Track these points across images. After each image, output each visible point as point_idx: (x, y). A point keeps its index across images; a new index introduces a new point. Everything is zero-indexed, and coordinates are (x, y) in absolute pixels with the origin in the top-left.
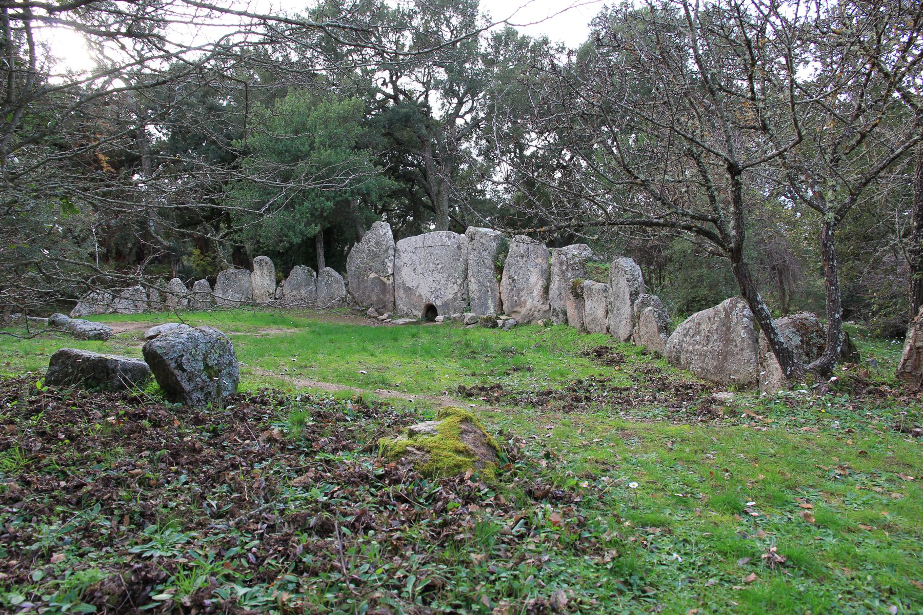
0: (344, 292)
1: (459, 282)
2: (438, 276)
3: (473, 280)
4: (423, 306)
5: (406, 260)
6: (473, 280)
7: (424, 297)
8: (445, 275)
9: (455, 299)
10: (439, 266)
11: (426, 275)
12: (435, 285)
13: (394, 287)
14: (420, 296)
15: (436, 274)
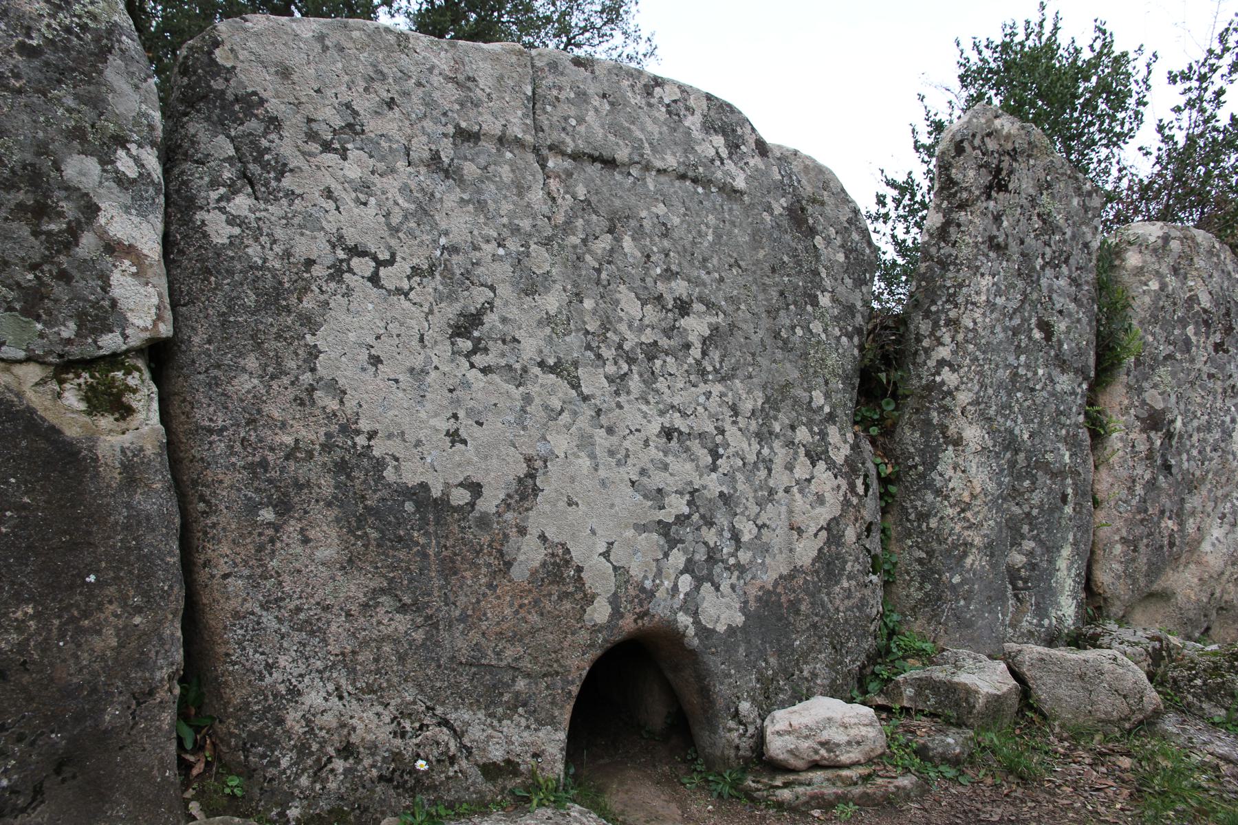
3: (973, 434)
4: (578, 664)
7: (599, 576)
10: (696, 326)
11: (594, 382)
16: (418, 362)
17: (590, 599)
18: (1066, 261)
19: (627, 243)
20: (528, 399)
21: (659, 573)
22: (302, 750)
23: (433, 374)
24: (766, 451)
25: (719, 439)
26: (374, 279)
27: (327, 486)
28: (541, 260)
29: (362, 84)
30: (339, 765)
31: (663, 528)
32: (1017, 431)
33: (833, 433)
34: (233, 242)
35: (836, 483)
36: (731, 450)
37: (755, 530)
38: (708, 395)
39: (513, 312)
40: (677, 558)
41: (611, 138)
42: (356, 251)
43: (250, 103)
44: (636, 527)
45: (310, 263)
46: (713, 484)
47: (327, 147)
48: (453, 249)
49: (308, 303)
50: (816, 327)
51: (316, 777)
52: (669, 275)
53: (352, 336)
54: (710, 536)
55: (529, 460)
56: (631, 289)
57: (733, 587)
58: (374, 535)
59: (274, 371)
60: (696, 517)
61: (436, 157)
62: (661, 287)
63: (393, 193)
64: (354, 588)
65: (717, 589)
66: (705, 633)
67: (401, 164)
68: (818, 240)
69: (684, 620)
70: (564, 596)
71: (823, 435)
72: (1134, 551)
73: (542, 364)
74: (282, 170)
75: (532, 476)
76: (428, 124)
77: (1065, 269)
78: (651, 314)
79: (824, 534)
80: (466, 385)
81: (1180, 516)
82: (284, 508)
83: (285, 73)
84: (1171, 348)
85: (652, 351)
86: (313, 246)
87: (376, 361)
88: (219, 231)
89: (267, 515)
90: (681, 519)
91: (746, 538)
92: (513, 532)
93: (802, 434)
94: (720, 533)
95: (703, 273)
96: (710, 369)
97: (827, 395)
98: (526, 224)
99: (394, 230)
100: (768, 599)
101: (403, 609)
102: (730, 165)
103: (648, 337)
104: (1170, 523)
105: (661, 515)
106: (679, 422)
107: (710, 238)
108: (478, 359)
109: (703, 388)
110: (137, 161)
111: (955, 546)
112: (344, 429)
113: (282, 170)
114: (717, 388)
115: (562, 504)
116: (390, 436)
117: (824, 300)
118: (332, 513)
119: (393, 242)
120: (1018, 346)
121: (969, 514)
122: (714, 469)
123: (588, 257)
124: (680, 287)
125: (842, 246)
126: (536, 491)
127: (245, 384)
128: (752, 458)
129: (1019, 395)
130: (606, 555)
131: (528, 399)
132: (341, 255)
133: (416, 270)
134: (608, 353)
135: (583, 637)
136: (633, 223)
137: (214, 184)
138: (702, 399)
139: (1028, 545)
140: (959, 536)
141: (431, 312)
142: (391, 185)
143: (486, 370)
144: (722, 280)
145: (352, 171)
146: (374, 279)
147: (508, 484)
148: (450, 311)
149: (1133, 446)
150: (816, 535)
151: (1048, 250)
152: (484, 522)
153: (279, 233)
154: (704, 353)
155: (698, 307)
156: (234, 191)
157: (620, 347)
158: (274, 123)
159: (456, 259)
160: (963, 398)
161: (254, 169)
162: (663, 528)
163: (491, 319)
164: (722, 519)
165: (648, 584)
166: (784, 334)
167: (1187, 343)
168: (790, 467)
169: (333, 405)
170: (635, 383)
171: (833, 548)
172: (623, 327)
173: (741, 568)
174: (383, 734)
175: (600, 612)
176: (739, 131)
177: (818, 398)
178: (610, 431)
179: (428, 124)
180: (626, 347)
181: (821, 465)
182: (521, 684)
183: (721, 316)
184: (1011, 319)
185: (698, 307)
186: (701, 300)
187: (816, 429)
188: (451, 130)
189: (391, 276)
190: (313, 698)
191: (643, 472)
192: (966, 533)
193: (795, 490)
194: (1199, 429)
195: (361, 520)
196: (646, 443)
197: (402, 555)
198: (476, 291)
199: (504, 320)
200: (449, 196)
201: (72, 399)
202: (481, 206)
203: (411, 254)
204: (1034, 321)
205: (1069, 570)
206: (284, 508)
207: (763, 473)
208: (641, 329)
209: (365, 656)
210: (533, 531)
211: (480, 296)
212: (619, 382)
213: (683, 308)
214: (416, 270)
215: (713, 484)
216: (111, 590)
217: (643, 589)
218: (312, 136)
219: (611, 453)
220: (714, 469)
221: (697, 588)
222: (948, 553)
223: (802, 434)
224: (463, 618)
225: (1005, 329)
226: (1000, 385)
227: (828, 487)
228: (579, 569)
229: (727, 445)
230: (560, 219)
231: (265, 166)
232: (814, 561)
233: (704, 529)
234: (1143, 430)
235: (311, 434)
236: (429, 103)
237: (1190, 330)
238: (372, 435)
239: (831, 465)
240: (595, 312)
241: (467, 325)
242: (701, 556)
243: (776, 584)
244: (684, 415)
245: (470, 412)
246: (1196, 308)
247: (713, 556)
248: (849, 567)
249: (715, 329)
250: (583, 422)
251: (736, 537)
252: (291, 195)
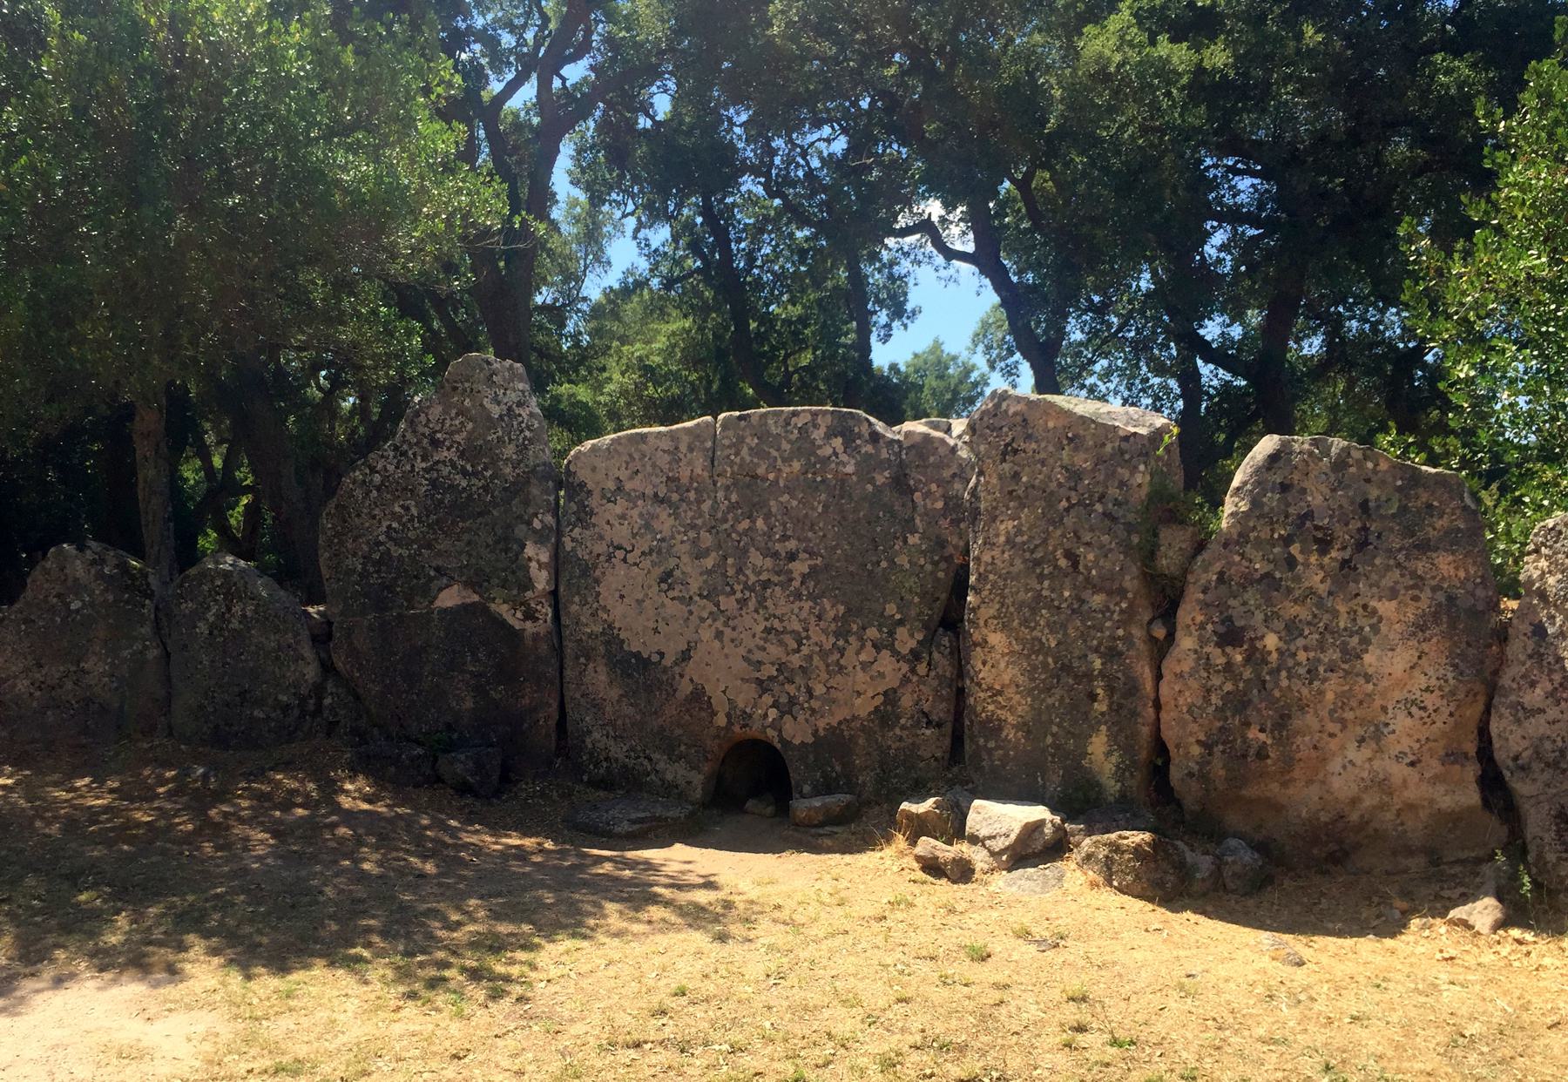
0: (311, 672)
1: (907, 640)
2: (795, 614)
3: (996, 639)
5: (621, 533)
6: (996, 639)
8: (832, 610)
9: (886, 714)
10: (800, 567)
12: (775, 651)
13: (559, 651)
14: (698, 696)
15: (778, 600)
16: (640, 596)
17: (714, 714)
18: (1101, 498)
19: (760, 523)
20: (691, 613)
21: (755, 706)
22: (591, 754)
23: (648, 602)
24: (841, 643)
25: (804, 635)
26: (625, 560)
27: (602, 649)
28: (707, 539)
29: (624, 465)
30: (605, 764)
31: (759, 682)
32: (1044, 640)
33: (902, 632)
34: (574, 549)
35: (898, 666)
36: (812, 641)
37: (825, 690)
38: (801, 609)
39: (688, 569)
40: (767, 699)
41: (755, 460)
42: (619, 548)
43: (582, 485)
44: (742, 679)
45: (599, 555)
46: (796, 660)
47: (609, 501)
48: (663, 540)
49: (598, 573)
50: (902, 560)
51: (595, 767)
52: (785, 538)
53: (614, 586)
54: (791, 689)
55: (689, 643)
56: (757, 549)
57: (807, 720)
58: (619, 672)
59: (584, 603)
60: (781, 678)
61: (656, 495)
62: (778, 546)
63: (636, 517)
64: (614, 693)
65: (795, 719)
66: (786, 743)
67: (640, 502)
68: (917, 495)
69: (771, 733)
70: (701, 709)
71: (891, 633)
72: (1209, 754)
73: (700, 595)
74: (592, 513)
75: (689, 650)
76: (653, 478)
77: (1099, 507)
78: (769, 562)
79: (881, 698)
80: (663, 605)
82: (588, 658)
83: (594, 469)
84: (1272, 566)
85: (766, 584)
86: (601, 548)
87: (622, 597)
88: (569, 545)
89: (582, 660)
90: (771, 678)
91: (817, 693)
92: (677, 677)
93: (872, 633)
94: (798, 689)
95: (810, 534)
96: (805, 593)
97: (899, 610)
98: (699, 522)
99: (634, 535)
100: (831, 729)
101: (631, 705)
102: (844, 457)
103: (764, 577)
104: (1262, 736)
105: (758, 675)
106: (776, 624)
107: (820, 510)
108: (671, 594)
109: (797, 603)
110: (541, 521)
111: (989, 720)
112: (609, 626)
113: (592, 513)
114: (807, 605)
115: (703, 665)
116: (626, 630)
117: (913, 539)
118: (604, 661)
119: (634, 541)
120: (1041, 574)
121: (1000, 699)
122: (798, 651)
123: (734, 535)
124: (792, 545)
125: (943, 496)
126: (690, 658)
127: (574, 608)
128: (828, 646)
129: (1044, 611)
130: (724, 692)
131: (691, 613)
132: (611, 550)
133: (643, 553)
134: (738, 587)
135: (713, 731)
136: (765, 510)
137: (568, 525)
138: (796, 611)
139: (1055, 729)
140: (993, 713)
141: (649, 572)
142: (635, 513)
143: (672, 599)
144: (824, 536)
145: (618, 510)
146: (625, 560)
147: (677, 653)
148: (658, 571)
149: (1208, 659)
150: (873, 697)
151: (1073, 494)
152: (665, 670)
153: (589, 544)
154: (802, 583)
155: (803, 556)
156: (575, 526)
157: (746, 583)
158: (590, 493)
159: (664, 544)
160: (987, 612)
161: (582, 515)
162: (759, 682)
163: (677, 573)
164: (798, 680)
165: (748, 710)
166: (869, 567)
167: (1291, 562)
168: (858, 653)
169: (605, 616)
170: (752, 604)
171: (889, 708)
172: (747, 572)
173: (813, 711)
174: (621, 756)
175: (721, 720)
176: (856, 430)
177: (891, 609)
178: (734, 629)
179: (653, 478)
180: (750, 583)
181: (886, 653)
182: (683, 748)
183: (820, 559)
184: (1032, 552)
185: (803, 556)
186: (805, 551)
187: (885, 630)
188: (664, 479)
189: (631, 558)
190: (596, 735)
191: (750, 651)
192: (999, 712)
193: (858, 668)
194: (1306, 649)
195: (615, 666)
196: (754, 636)
197: (630, 681)
198: (671, 560)
199: (683, 573)
200: (663, 513)
201: (519, 615)
202: (676, 516)
203: (643, 544)
204: (1059, 553)
205: (1109, 754)
206: (588, 658)
207: (836, 656)
208: (760, 573)
209: (619, 722)
210: (687, 678)
211: (672, 562)
212: (743, 602)
213: (792, 557)
214: (643, 553)
215: (796, 660)
216: (527, 684)
217: (745, 713)
218: (604, 496)
219: (732, 641)
220: (798, 651)
221: (781, 717)
222: (983, 724)
223: (872, 633)
224: (656, 713)
225: (1025, 561)
226: (1022, 604)
227: (890, 668)
228: (710, 698)
229: (808, 638)
230: (719, 515)
231: (586, 513)
232: (870, 714)
233: (786, 686)
234: (1218, 645)
235: (598, 629)
236: (654, 466)
237: (1295, 549)
238: (620, 629)
239: (895, 653)
240: (733, 565)
241: (666, 577)
242: (784, 700)
243: (840, 723)
244: (781, 621)
245: (663, 619)
246: (1308, 524)
247: (792, 701)
248: (903, 721)
249: (813, 568)
250: (719, 624)
251: (810, 692)
252: (594, 525)
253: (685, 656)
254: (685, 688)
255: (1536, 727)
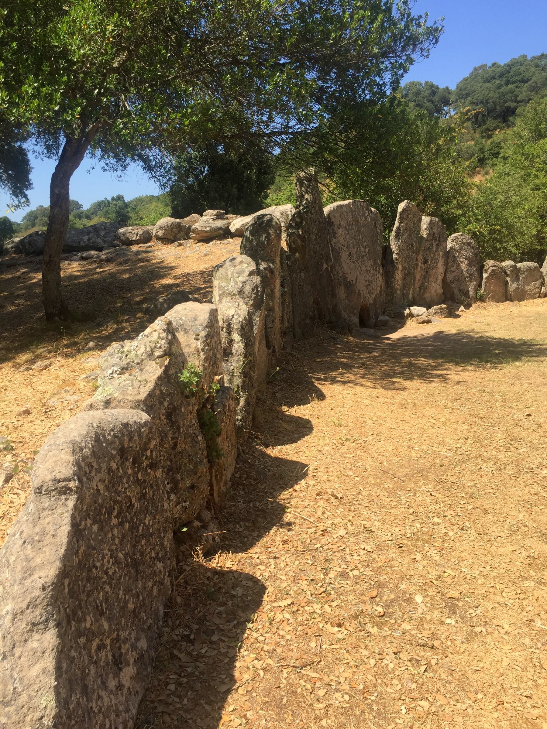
3: (400, 267)
14: (359, 294)
43: (333, 222)
81: (428, 282)
86: (340, 246)
88: (333, 245)
253: (356, 282)
254: (357, 291)
255: (454, 274)
